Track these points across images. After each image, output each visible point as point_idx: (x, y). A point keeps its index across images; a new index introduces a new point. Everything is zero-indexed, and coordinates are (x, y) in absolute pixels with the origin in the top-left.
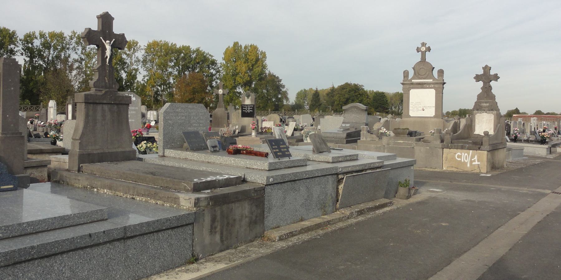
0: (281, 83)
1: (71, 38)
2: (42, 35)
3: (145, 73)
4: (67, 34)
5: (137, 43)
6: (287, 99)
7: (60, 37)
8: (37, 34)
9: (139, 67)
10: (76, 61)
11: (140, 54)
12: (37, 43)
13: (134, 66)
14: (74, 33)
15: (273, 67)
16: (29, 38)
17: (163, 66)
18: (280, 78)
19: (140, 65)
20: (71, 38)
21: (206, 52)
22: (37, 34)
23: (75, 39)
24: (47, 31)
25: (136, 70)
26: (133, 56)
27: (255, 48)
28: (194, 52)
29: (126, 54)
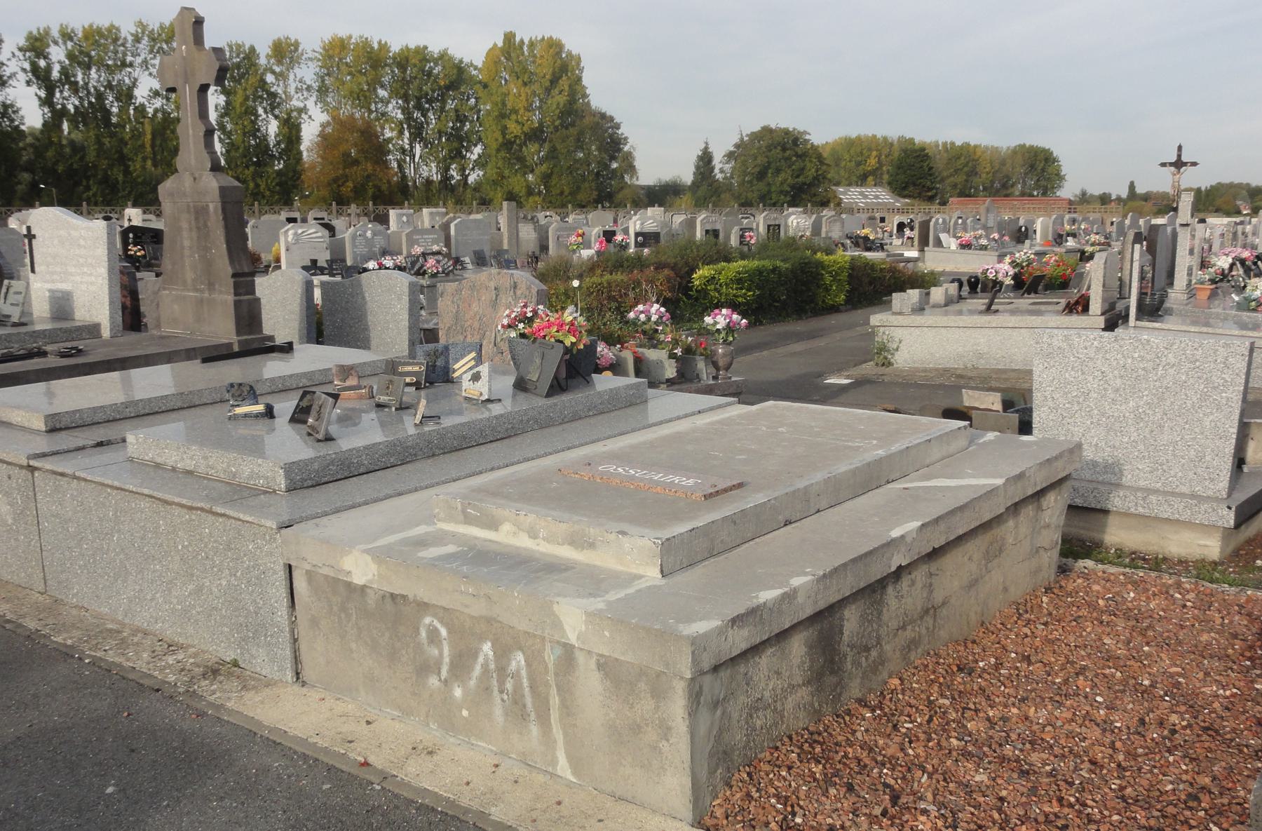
0: (620, 132)
1: (137, 40)
2: (67, 36)
3: (324, 117)
4: (127, 29)
5: (297, 44)
6: (631, 168)
7: (112, 35)
8: (55, 33)
9: (310, 104)
10: (156, 94)
11: (307, 72)
12: (58, 54)
13: (296, 103)
14: (140, 24)
15: (601, 93)
16: (36, 46)
17: (363, 98)
18: (617, 120)
19: (314, 99)
20: (137, 40)
21: (466, 60)
22: (55, 33)
23: (145, 41)
24: (78, 24)
25: (303, 110)
26: (291, 77)
27: (555, 46)
28: (436, 61)
29: (273, 72)
